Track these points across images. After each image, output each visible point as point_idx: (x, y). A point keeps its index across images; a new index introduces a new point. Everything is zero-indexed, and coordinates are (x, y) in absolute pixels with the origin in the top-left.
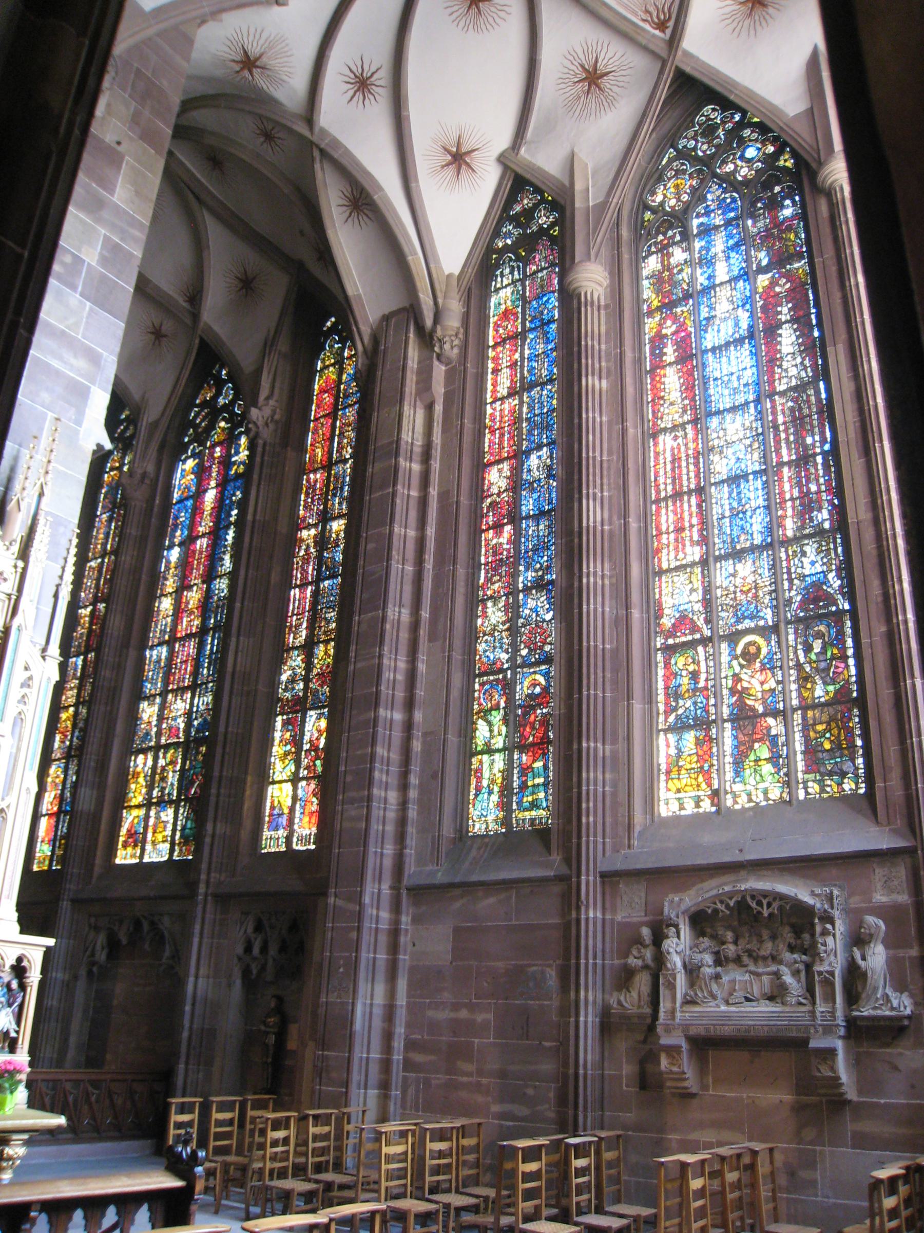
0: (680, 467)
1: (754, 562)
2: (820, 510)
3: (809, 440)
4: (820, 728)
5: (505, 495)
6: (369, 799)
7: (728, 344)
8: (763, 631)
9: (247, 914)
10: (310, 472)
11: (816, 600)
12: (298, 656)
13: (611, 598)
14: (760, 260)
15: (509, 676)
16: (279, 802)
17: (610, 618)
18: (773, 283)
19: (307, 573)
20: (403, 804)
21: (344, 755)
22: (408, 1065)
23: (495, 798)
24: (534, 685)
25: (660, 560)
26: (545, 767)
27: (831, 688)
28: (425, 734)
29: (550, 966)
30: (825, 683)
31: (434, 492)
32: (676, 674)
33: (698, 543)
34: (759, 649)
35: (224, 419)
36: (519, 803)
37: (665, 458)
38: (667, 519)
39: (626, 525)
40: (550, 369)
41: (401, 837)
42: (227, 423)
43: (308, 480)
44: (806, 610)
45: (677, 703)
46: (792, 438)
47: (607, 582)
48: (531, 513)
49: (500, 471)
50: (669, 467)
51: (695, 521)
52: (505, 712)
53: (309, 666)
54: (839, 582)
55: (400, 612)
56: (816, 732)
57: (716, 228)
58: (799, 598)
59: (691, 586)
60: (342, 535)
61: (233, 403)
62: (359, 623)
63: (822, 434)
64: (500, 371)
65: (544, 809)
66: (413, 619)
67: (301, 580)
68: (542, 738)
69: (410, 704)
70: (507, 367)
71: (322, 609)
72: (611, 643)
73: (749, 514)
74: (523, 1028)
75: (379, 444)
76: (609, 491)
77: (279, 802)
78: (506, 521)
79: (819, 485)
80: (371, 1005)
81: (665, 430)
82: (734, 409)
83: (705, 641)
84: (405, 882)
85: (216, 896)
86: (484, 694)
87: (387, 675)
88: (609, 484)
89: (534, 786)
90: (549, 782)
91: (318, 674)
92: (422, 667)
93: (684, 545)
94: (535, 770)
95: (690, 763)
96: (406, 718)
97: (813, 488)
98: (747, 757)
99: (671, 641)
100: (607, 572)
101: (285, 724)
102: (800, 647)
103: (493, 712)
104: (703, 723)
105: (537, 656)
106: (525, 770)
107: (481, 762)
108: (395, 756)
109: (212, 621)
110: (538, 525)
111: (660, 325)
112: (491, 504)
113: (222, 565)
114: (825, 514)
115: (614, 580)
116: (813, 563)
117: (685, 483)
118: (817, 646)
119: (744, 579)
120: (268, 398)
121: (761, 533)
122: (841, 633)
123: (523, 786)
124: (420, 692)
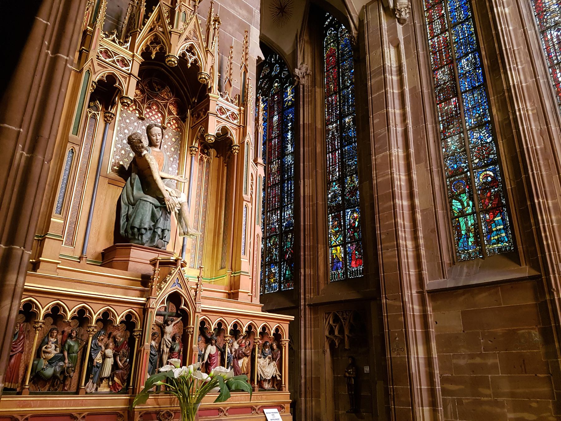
6: (398, 245)
9: (329, 313)
10: (329, 97)
12: (336, 185)
13: (535, 121)
15: (469, 174)
17: (537, 132)
19: (335, 145)
20: (417, 248)
22: (444, 391)
23: (471, 240)
24: (486, 176)
26: (503, 219)
28: (421, 211)
29: (533, 329)
31: (407, 89)
35: (277, 82)
36: (489, 241)
39: (537, 81)
40: (465, 13)
41: (419, 265)
42: (278, 83)
43: (328, 101)
47: (530, 113)
48: (467, 89)
49: (443, 72)
52: (470, 194)
53: (343, 189)
55: (398, 151)
60: (352, 123)
61: (280, 73)
62: (375, 159)
64: (434, 21)
65: (507, 242)
66: (405, 154)
67: (332, 149)
68: (497, 204)
69: (411, 196)
70: (438, 19)
71: (346, 161)
72: (540, 145)
74: (521, 366)
75: (372, 69)
76: (521, 65)
80: (418, 358)
84: (426, 288)
85: (309, 305)
86: (453, 186)
87: (397, 183)
88: (521, 61)
89: (497, 230)
90: (507, 228)
91: (349, 191)
92: (415, 177)
94: (496, 222)
96: (410, 204)
100: (529, 108)
101: (333, 218)
103: (462, 195)
105: (485, 162)
106: (489, 223)
107: (458, 221)
108: (407, 224)
109: (286, 176)
110: (473, 95)
113: (287, 150)
115: (535, 111)
120: (302, 64)
123: (490, 232)
124: (416, 190)
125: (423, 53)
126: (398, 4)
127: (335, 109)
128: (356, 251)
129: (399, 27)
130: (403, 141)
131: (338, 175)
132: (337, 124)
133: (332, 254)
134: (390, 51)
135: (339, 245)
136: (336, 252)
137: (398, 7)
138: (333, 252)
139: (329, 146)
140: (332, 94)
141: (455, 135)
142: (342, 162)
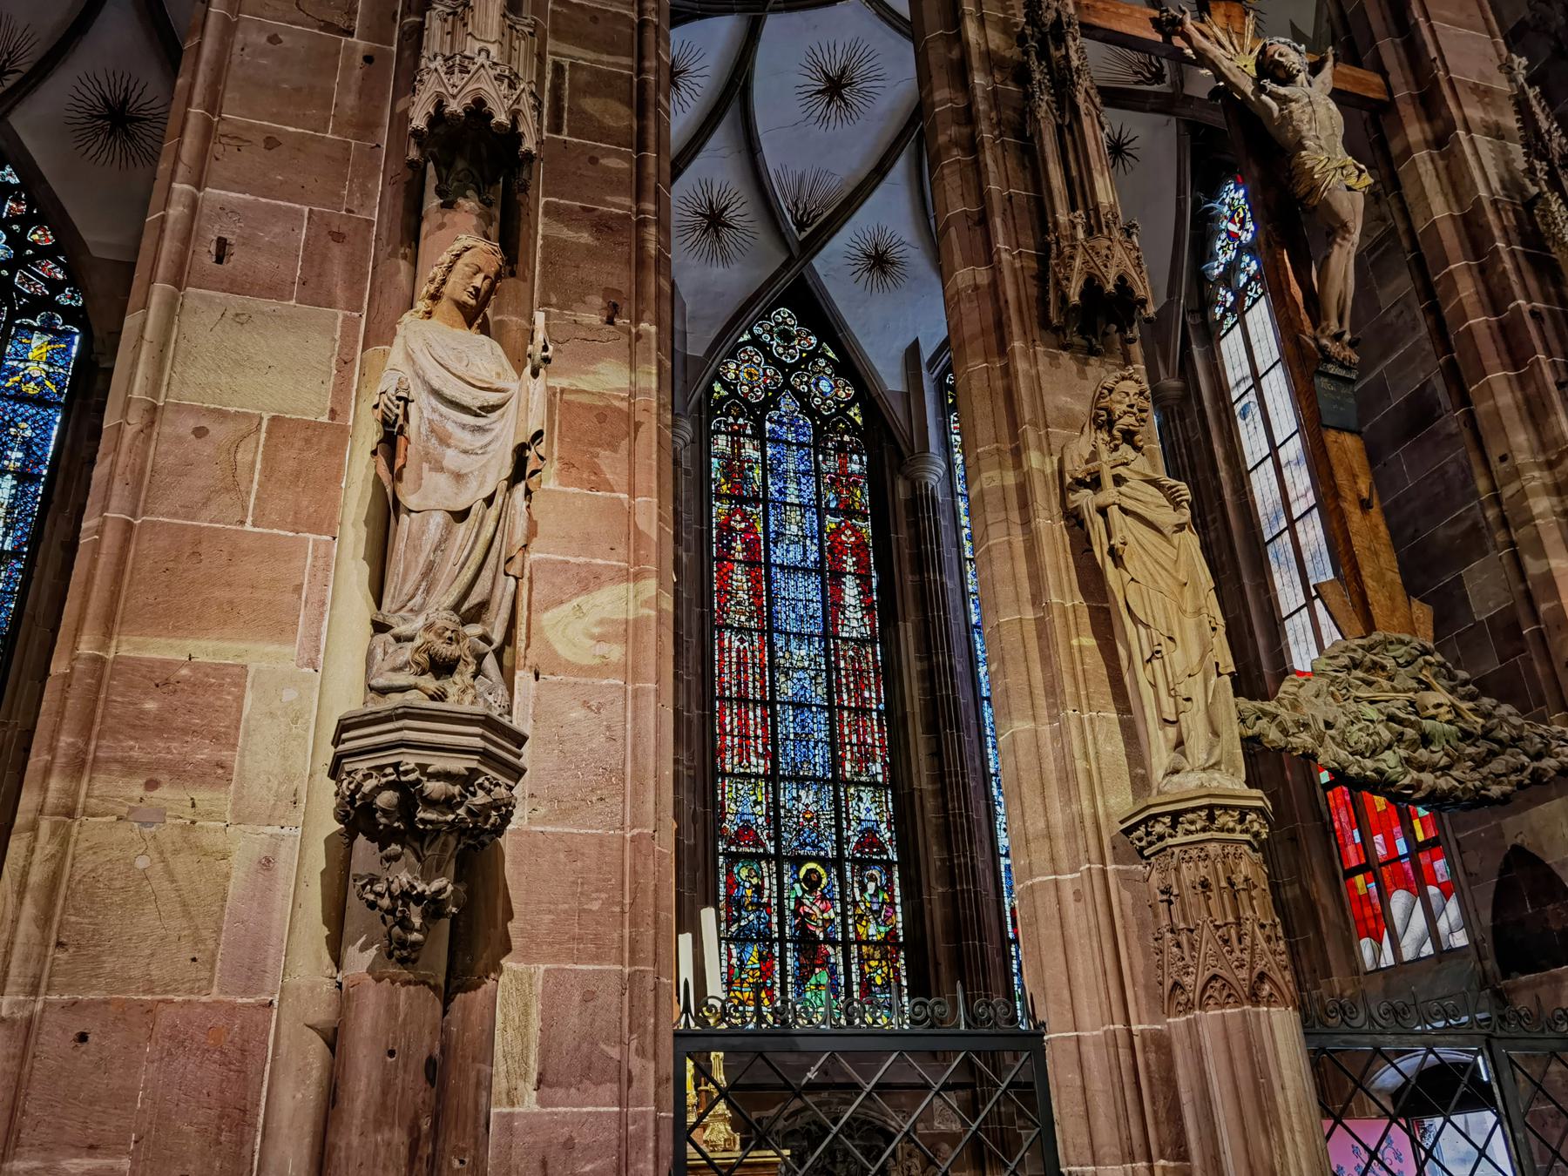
0: (746, 671)
1: (816, 793)
2: (874, 762)
3: (867, 694)
4: (873, 963)
7: (796, 569)
8: (822, 861)
11: (871, 846)
14: (829, 501)
18: (838, 531)
25: (723, 760)
27: (882, 929)
30: (877, 923)
32: (738, 884)
33: (763, 756)
34: (820, 878)
37: (730, 657)
38: (730, 721)
44: (862, 853)
45: (740, 914)
46: (852, 686)
50: (734, 667)
51: (759, 732)
54: (889, 834)
56: (870, 967)
57: (789, 444)
58: (856, 839)
59: (754, 798)
63: (878, 692)
73: (812, 744)
79: (874, 739)
81: (730, 627)
82: (799, 636)
83: (766, 856)
93: (748, 754)
95: (753, 977)
97: (869, 741)
98: (808, 979)
99: (733, 849)
102: (856, 885)
104: (764, 938)
111: (730, 516)
114: (878, 766)
116: (869, 810)
117: (750, 690)
118: (871, 887)
119: (807, 806)
121: (824, 767)
122: (890, 880)
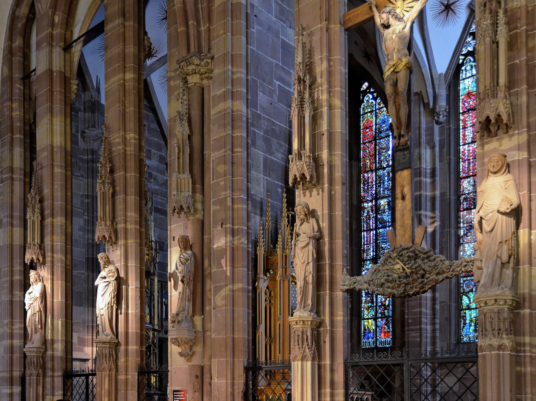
5: (471, 194)
16: (368, 327)
21: (407, 311)
77: (368, 327)
78: (472, 207)
112: (464, 198)
125: (454, 158)
126: (437, 107)
127: (371, 187)
128: (385, 325)
129: (436, 128)
130: (431, 240)
131: (372, 255)
132: (372, 204)
133: (364, 325)
134: (426, 152)
135: (371, 319)
136: (367, 324)
137: (437, 110)
138: (365, 324)
139: (364, 224)
140: (368, 171)
141: (471, 243)
142: (376, 242)
